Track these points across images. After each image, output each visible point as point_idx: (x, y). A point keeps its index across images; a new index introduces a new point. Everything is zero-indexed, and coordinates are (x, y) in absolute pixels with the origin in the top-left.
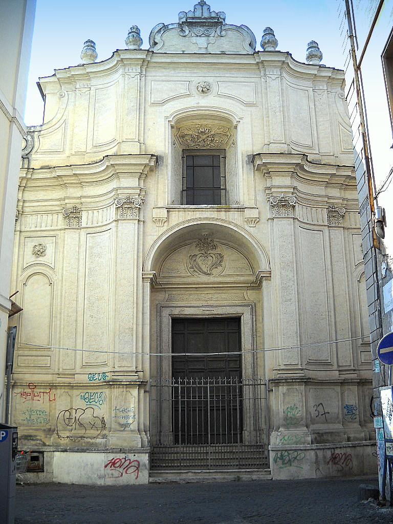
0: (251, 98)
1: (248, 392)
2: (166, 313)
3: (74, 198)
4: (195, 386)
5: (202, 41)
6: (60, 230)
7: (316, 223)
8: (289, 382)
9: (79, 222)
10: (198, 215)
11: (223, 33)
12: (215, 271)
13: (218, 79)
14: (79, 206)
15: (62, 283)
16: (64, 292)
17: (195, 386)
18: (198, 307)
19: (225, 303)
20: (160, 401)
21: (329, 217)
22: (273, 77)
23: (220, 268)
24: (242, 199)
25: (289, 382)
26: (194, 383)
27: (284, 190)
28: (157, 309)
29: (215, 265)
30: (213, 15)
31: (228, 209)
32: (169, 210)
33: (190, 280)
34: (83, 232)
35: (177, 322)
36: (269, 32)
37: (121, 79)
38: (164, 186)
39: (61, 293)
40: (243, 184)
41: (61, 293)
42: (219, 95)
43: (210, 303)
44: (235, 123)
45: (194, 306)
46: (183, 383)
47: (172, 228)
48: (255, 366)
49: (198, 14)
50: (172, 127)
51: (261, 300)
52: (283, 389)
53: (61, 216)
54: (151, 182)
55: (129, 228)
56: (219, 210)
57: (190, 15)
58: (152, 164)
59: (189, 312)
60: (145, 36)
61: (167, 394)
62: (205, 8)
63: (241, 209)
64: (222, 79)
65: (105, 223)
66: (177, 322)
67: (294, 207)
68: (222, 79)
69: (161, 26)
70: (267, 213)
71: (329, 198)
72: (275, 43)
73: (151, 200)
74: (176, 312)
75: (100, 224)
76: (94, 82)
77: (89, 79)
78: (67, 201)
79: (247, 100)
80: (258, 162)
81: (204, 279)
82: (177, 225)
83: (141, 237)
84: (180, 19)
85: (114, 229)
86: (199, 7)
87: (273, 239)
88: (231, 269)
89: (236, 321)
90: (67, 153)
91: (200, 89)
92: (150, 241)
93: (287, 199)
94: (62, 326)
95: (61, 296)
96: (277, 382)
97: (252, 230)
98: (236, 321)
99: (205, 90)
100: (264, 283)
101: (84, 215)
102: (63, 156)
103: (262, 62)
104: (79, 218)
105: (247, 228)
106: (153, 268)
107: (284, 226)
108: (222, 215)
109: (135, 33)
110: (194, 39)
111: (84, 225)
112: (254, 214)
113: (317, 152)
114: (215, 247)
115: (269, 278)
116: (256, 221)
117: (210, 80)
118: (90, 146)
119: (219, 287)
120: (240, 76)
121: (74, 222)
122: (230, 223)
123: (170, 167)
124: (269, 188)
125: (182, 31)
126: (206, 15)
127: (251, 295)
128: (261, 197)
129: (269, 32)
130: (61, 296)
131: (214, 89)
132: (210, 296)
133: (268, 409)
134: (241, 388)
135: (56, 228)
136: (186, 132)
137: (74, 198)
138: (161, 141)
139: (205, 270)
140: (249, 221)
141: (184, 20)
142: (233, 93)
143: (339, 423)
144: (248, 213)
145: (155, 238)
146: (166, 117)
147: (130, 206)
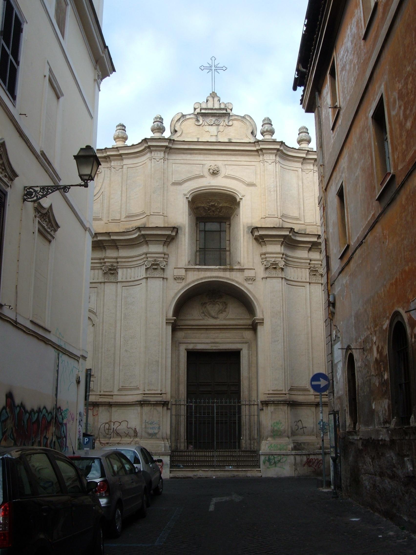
1: (245, 410)
4: (205, 405)
5: (213, 130)
6: (101, 283)
8: (276, 403)
9: (116, 277)
10: (208, 274)
11: (231, 123)
13: (226, 163)
14: (115, 264)
15: (103, 324)
16: (104, 332)
17: (205, 405)
18: (207, 343)
19: (229, 340)
20: (178, 415)
24: (242, 262)
25: (276, 403)
26: (204, 403)
27: (275, 256)
30: (223, 106)
31: (232, 270)
32: (187, 270)
33: (201, 322)
34: (119, 285)
36: (268, 122)
37: (148, 162)
39: (102, 332)
41: (102, 332)
42: (226, 177)
43: (217, 340)
44: (238, 200)
46: (196, 402)
48: (250, 390)
49: (210, 105)
50: (189, 202)
52: (271, 408)
56: (225, 270)
57: (204, 106)
58: (174, 234)
59: (200, 347)
60: (167, 124)
61: (183, 410)
62: (216, 99)
63: (242, 270)
65: (136, 279)
69: (180, 115)
70: (260, 272)
72: (272, 132)
73: (172, 260)
74: (191, 347)
75: (133, 279)
76: (126, 162)
77: (122, 160)
78: (106, 260)
79: (248, 180)
80: (256, 234)
82: (193, 282)
84: (195, 109)
86: (211, 99)
87: (264, 293)
90: (105, 220)
91: (211, 171)
93: (277, 262)
94: (103, 358)
95: (102, 334)
96: (266, 403)
97: (249, 287)
99: (215, 173)
100: (259, 328)
101: (120, 271)
102: (102, 222)
103: (261, 150)
106: (174, 316)
108: (227, 274)
110: (207, 128)
111: (120, 279)
112: (251, 274)
115: (262, 323)
116: (253, 279)
117: (220, 164)
118: (124, 215)
120: (243, 159)
121: (112, 278)
122: (233, 280)
123: (187, 235)
125: (198, 121)
126: (217, 106)
127: (248, 334)
128: (258, 259)
129: (268, 122)
130: (102, 334)
131: (223, 172)
133: (259, 423)
134: (240, 407)
138: (180, 215)
141: (198, 111)
143: (313, 435)
144: (247, 273)
146: (185, 195)
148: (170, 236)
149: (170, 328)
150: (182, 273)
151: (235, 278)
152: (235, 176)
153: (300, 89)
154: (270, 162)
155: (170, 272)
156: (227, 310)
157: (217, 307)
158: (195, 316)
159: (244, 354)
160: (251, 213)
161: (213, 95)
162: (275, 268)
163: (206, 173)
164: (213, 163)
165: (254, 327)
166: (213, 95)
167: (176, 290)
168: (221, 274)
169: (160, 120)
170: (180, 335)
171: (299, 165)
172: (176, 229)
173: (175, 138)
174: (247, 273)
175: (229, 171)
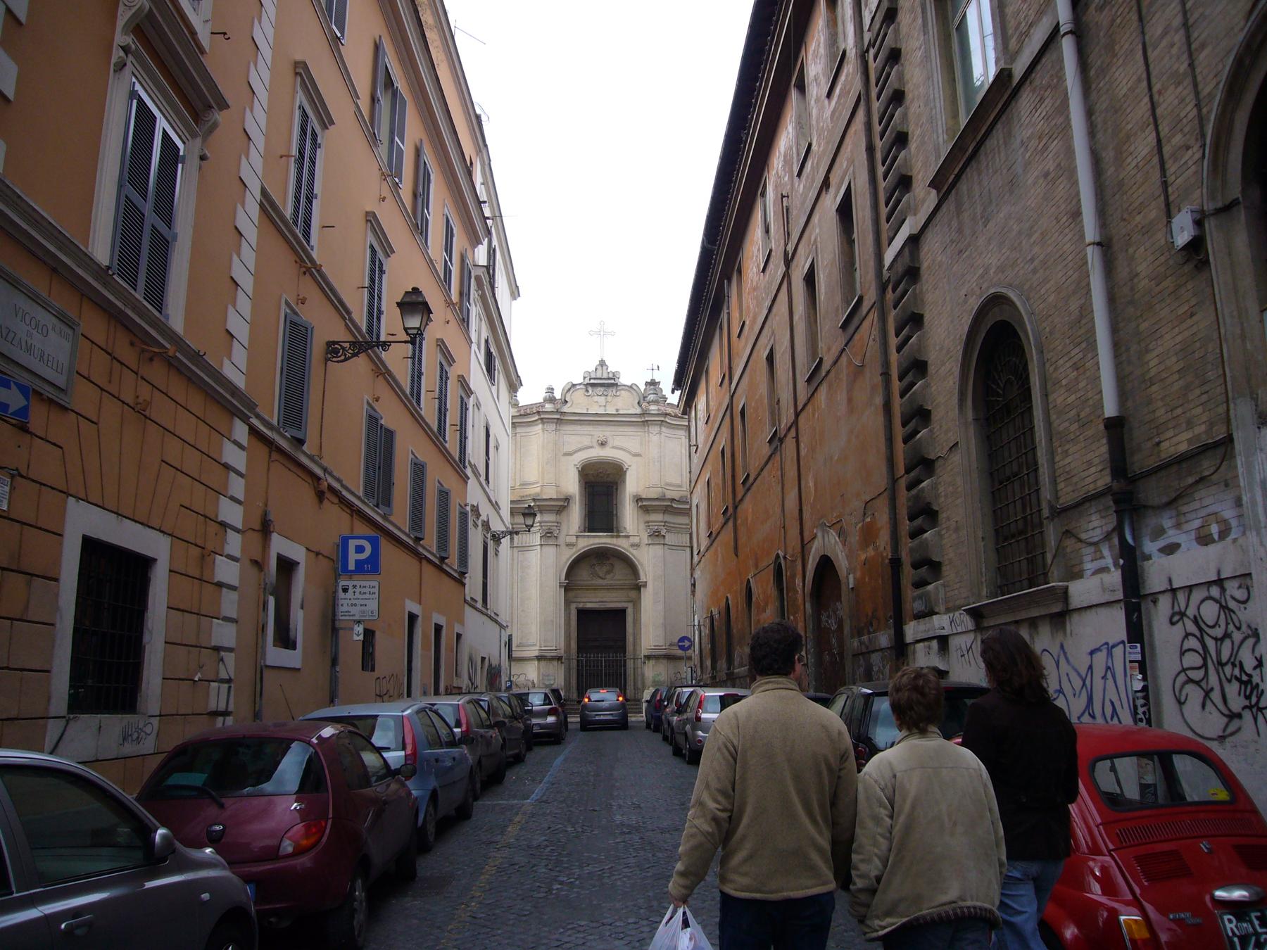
1: (630, 664)
5: (602, 400)
8: (657, 658)
10: (597, 540)
12: (608, 577)
25: (657, 658)
31: (618, 537)
32: (577, 537)
40: (629, 517)
49: (599, 375)
52: (652, 662)
55: (551, 551)
61: (574, 664)
63: (628, 537)
70: (645, 540)
87: (649, 559)
92: (564, 559)
96: (648, 657)
97: (634, 552)
99: (603, 444)
107: (657, 551)
108: (614, 541)
109: (550, 390)
110: (596, 398)
112: (636, 540)
116: (636, 546)
117: (607, 434)
119: (610, 588)
126: (605, 376)
128: (642, 526)
133: (643, 675)
138: (571, 485)
140: (632, 545)
141: (587, 381)
142: (625, 445)
144: (632, 540)
147: (549, 536)
148: (561, 506)
150: (573, 539)
151: (622, 544)
152: (621, 447)
153: (678, 393)
155: (562, 540)
157: (605, 569)
158: (584, 575)
160: (633, 485)
161: (602, 363)
163: (595, 444)
165: (638, 587)
166: (602, 363)
167: (569, 555)
168: (608, 540)
169: (550, 390)
170: (571, 594)
172: (567, 499)
173: (565, 409)
174: (632, 540)
175: (617, 441)
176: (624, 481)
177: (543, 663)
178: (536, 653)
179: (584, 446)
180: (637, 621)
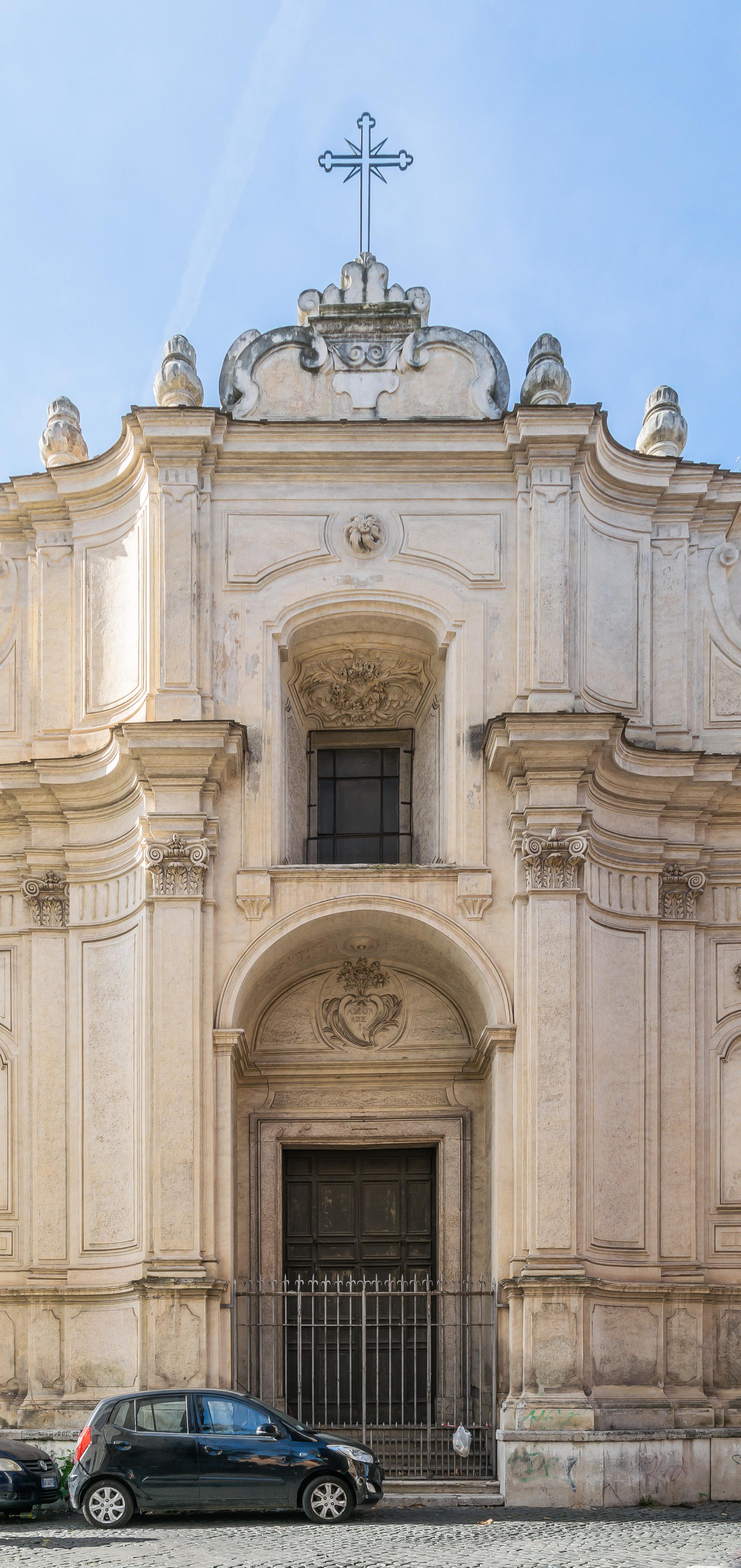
0: (484, 563)
2: (269, 1134)
3: (47, 851)
4: (332, 1294)
6: (20, 934)
7: (628, 910)
9: (64, 912)
10: (344, 889)
11: (424, 357)
13: (404, 507)
15: (30, 1063)
16: (35, 1083)
17: (332, 1294)
18: (341, 1120)
19: (403, 1111)
20: (255, 1328)
21: (663, 898)
22: (552, 493)
23: (393, 1031)
26: (332, 1288)
28: (249, 1125)
29: (381, 1023)
30: (396, 297)
33: (325, 1058)
35: (296, 1158)
36: (547, 350)
38: (265, 813)
39: (30, 1085)
40: (457, 802)
41: (30, 1085)
43: (370, 1111)
44: (441, 639)
45: (331, 1117)
46: (306, 1288)
47: (284, 923)
50: (283, 655)
51: (485, 1107)
52: (532, 1304)
53: (20, 900)
54: (232, 803)
55: (182, 920)
59: (320, 1131)
61: (272, 1312)
63: (451, 873)
64: (415, 507)
65: (124, 913)
66: (296, 1158)
67: (580, 864)
68: (415, 507)
69: (250, 339)
70: (511, 876)
71: (668, 845)
73: (232, 850)
74: (293, 1131)
75: (113, 917)
81: (356, 1053)
82: (297, 914)
83: (210, 945)
85: (144, 926)
88: (420, 1032)
89: (426, 1155)
91: (355, 537)
92: (230, 953)
93: (565, 843)
94: (35, 1163)
95: (30, 1094)
96: (516, 1287)
97: (473, 927)
98: (426, 1155)
99: (367, 541)
100: (498, 1058)
101: (75, 895)
104: (63, 904)
105: (461, 921)
106: (242, 1019)
107: (556, 914)
109: (182, 353)
111: (74, 919)
112: (481, 885)
113: (648, 723)
114: (382, 980)
115: (508, 1046)
117: (383, 510)
121: (52, 913)
124: (520, 816)
125: (308, 353)
127: (460, 1094)
128: (501, 840)
130: (30, 1094)
131: (393, 533)
132: (369, 1096)
134: (434, 1299)
135: (11, 930)
136: (317, 675)
137: (47, 851)
139: (359, 1034)
140: (467, 903)
144: (467, 885)
145: (243, 947)
146: (268, 625)
149: (227, 1061)
154: (552, 493)
155: (227, 884)
156: (400, 1019)
159: (450, 1150)
161: (365, 267)
162: (556, 862)
164: (360, 508)
166: (365, 267)
167: (250, 941)
169: (182, 353)
171: (641, 521)
176: (444, 679)
177: (158, 1306)
178: (138, 1273)
179: (297, 554)
180: (473, 1183)
